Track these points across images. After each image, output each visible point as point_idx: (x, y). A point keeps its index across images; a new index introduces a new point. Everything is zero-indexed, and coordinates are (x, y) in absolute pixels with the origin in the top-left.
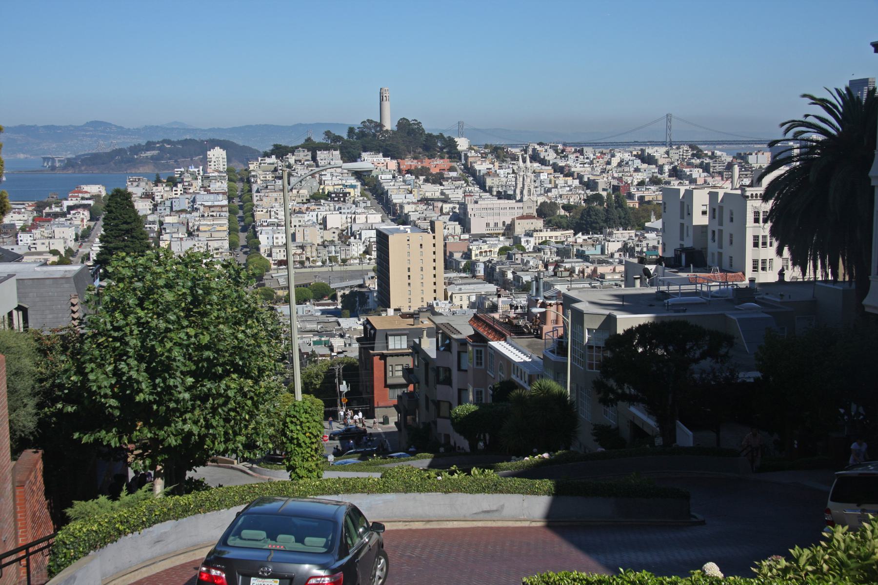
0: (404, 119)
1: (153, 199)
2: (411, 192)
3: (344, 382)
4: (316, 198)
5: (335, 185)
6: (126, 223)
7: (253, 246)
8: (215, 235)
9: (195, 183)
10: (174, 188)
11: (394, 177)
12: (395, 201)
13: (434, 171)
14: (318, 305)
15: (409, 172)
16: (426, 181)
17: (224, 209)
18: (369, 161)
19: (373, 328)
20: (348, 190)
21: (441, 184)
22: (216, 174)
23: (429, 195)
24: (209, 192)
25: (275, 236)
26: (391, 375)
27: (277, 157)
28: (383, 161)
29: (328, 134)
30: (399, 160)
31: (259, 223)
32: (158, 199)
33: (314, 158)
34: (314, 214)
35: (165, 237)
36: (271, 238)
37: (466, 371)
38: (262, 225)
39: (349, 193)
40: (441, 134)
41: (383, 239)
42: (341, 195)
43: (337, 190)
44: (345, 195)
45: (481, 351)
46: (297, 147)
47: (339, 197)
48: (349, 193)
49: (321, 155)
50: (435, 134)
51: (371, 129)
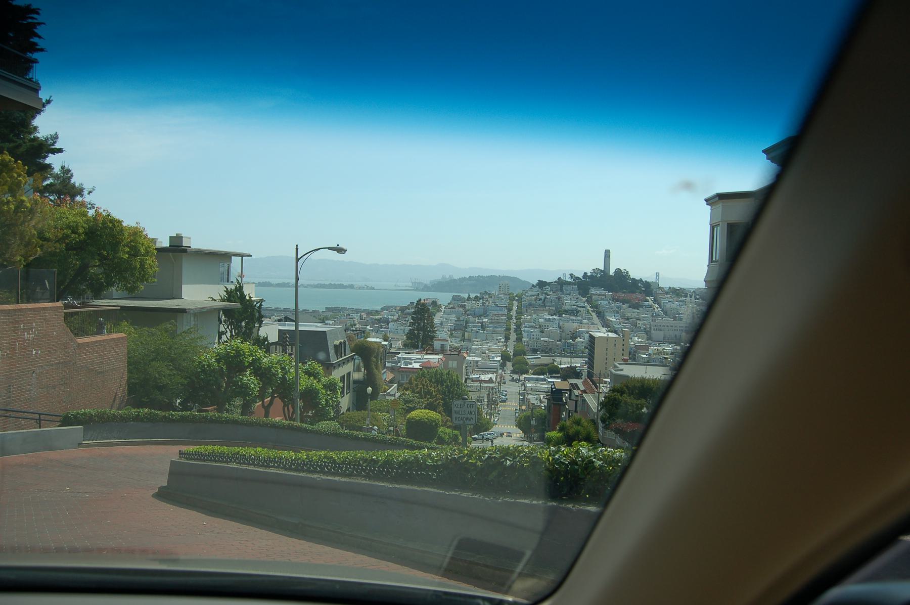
0: (618, 269)
1: (465, 308)
4: (559, 312)
10: (478, 302)
14: (551, 377)
19: (555, 388)
20: (579, 309)
21: (638, 309)
29: (571, 275)
32: (467, 308)
33: (561, 290)
35: (469, 329)
38: (525, 327)
39: (580, 311)
44: (578, 312)
46: (552, 282)
47: (574, 312)
48: (580, 311)
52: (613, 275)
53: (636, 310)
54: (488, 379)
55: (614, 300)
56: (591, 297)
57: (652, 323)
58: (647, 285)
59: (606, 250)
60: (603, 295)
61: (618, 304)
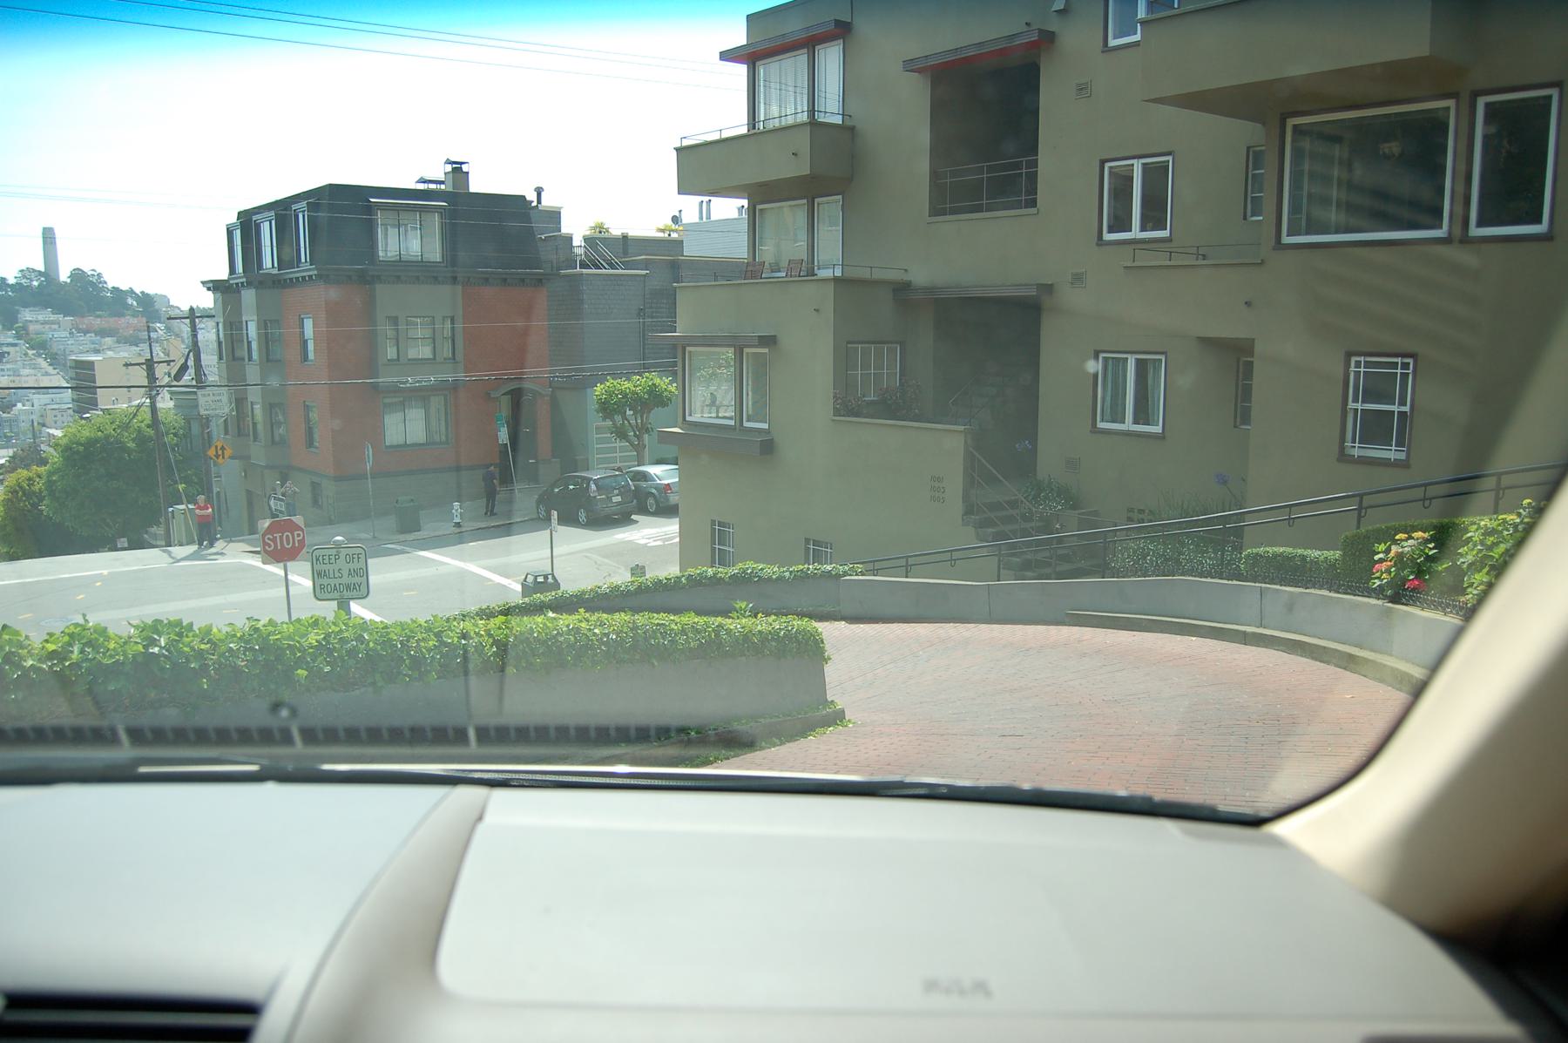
15: (86, 332)
53: (134, 348)
56: (25, 328)
58: (146, 301)
60: (53, 323)
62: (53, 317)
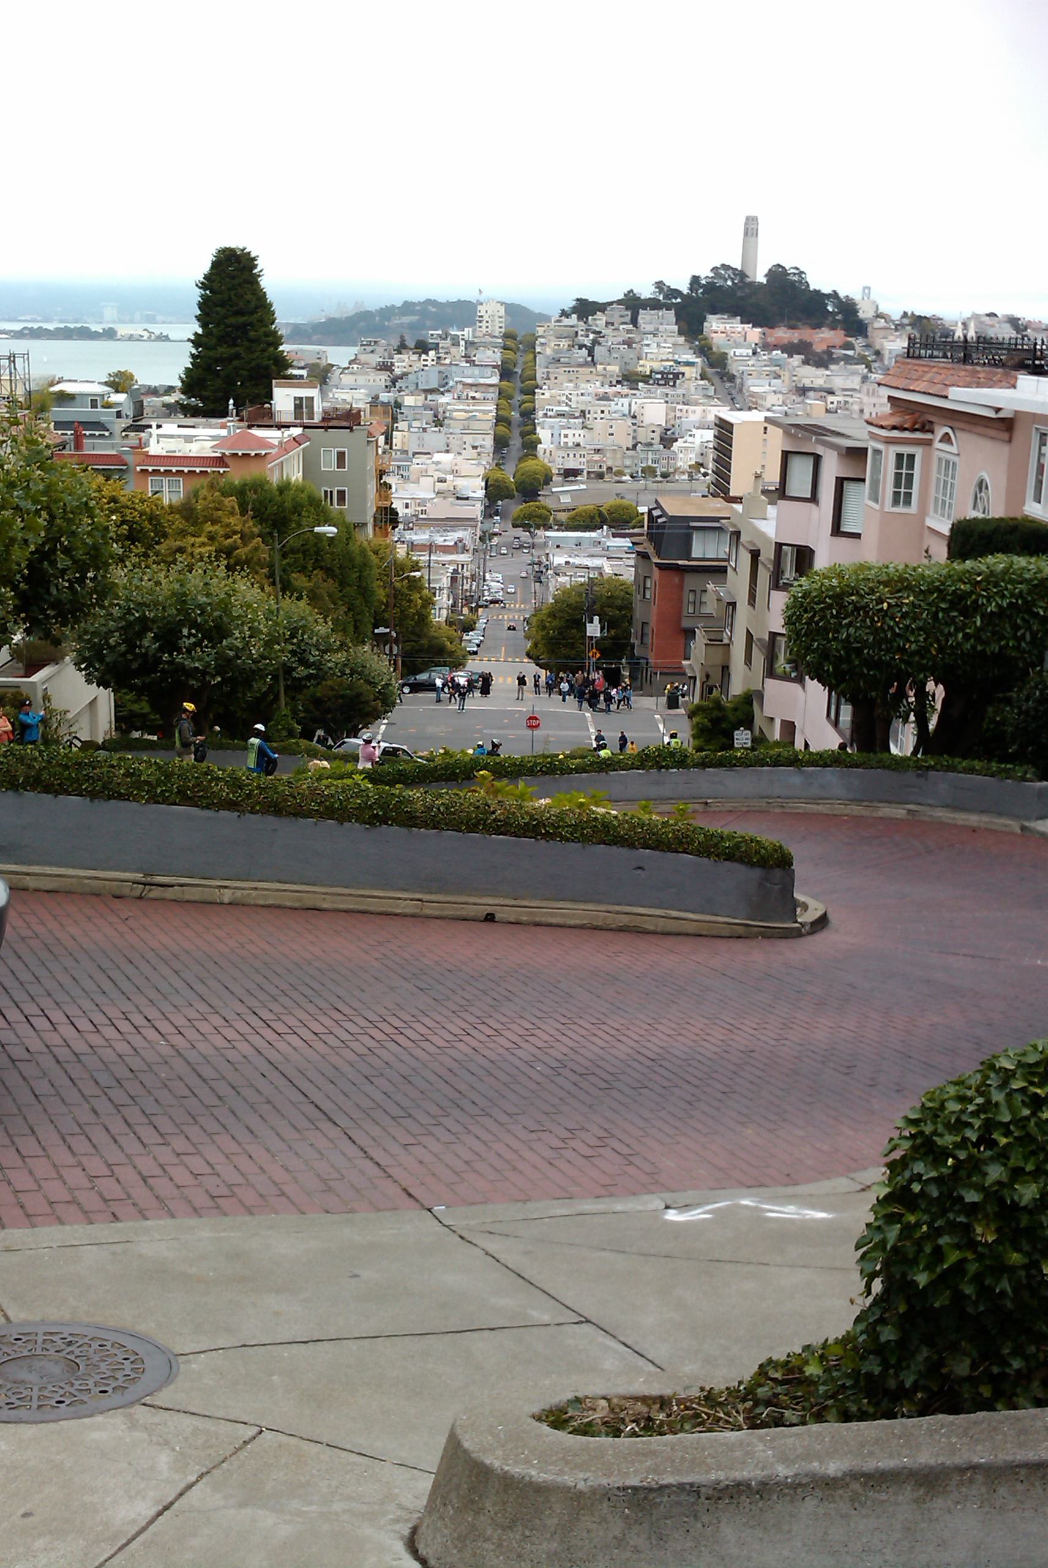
0: (779, 266)
2: (779, 377)
3: (596, 619)
4: (631, 379)
5: (662, 360)
6: (240, 313)
7: (531, 446)
8: (475, 425)
9: (453, 350)
10: (424, 357)
11: (754, 353)
12: (752, 389)
13: (819, 348)
14: (614, 536)
15: (776, 347)
16: (806, 362)
17: (491, 389)
18: (718, 327)
19: (664, 514)
20: (682, 369)
21: (827, 368)
22: (488, 339)
23: (807, 383)
24: (472, 363)
25: (564, 432)
26: (691, 610)
27: (579, 318)
28: (739, 329)
29: (659, 285)
30: (766, 329)
31: (540, 413)
32: (398, 371)
33: (634, 321)
34: (626, 401)
35: (402, 425)
36: (556, 435)
37: (857, 536)
39: (683, 374)
40: (834, 291)
41: (724, 430)
42: (671, 376)
43: (665, 368)
44: (676, 376)
45: (912, 457)
46: (611, 303)
47: (669, 378)
48: (683, 374)
49: (644, 316)
50: (826, 290)
51: (726, 280)
52: (764, 281)
54: (452, 544)
55: (767, 347)
57: (866, 399)
59: (748, 218)
61: (777, 353)
62: (740, 327)
